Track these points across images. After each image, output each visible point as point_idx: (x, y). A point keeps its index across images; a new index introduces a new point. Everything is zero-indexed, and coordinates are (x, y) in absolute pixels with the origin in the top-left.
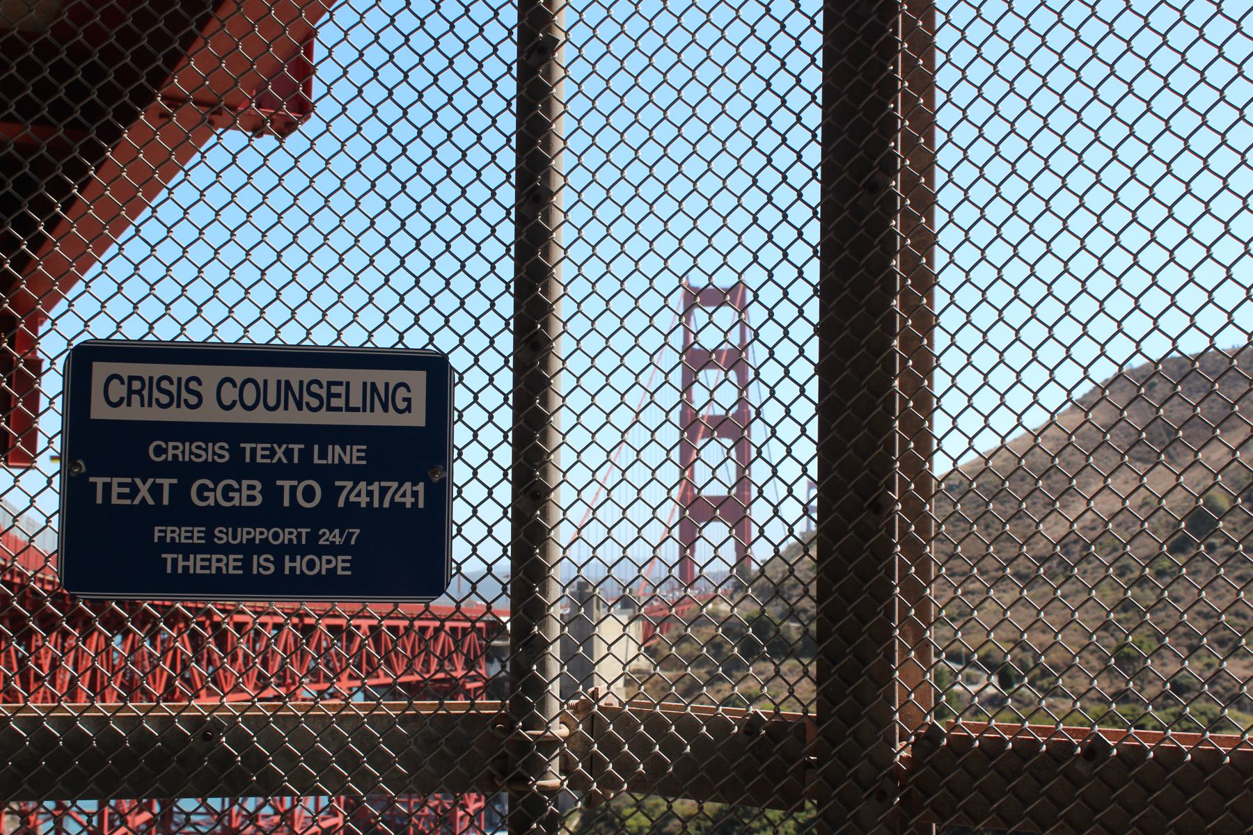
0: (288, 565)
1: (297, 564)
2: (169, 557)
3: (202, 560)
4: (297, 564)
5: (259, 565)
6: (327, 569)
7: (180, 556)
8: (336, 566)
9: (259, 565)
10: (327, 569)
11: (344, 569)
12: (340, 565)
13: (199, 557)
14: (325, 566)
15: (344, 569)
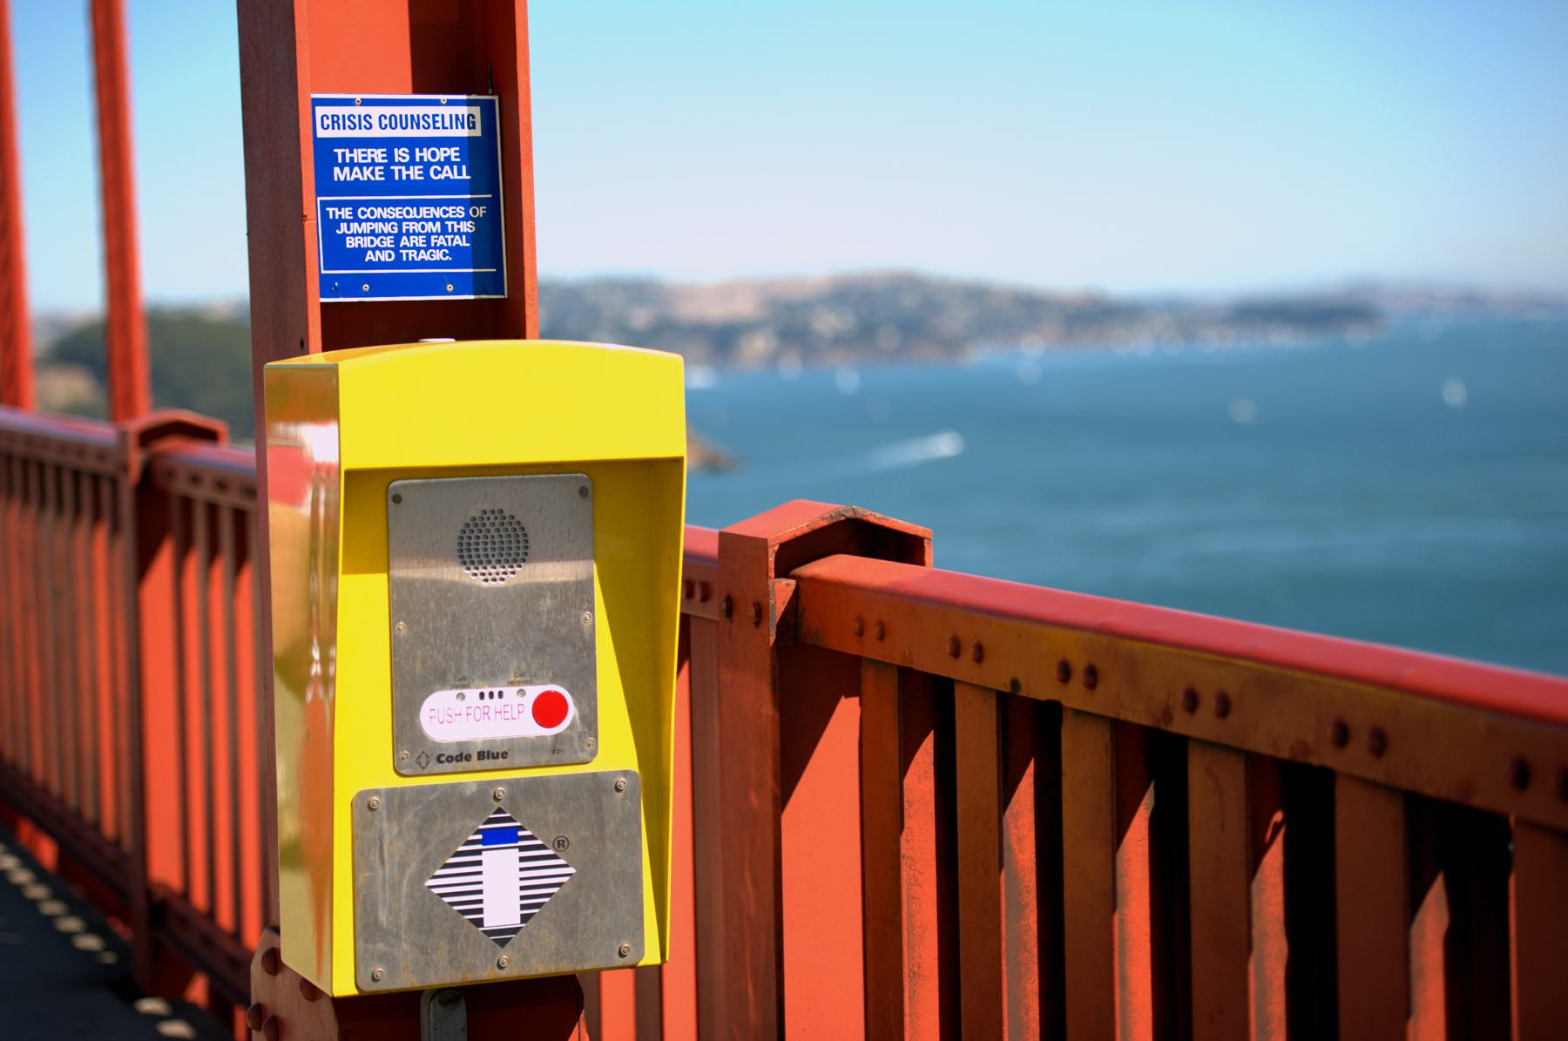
0: (418, 154)
1: (424, 154)
2: (339, 151)
3: (363, 153)
4: (424, 154)
5: (399, 156)
6: (445, 158)
7: (347, 151)
8: (450, 156)
9: (399, 156)
10: (445, 158)
11: (456, 157)
12: (453, 155)
13: (360, 150)
14: (443, 155)
15: (456, 157)
